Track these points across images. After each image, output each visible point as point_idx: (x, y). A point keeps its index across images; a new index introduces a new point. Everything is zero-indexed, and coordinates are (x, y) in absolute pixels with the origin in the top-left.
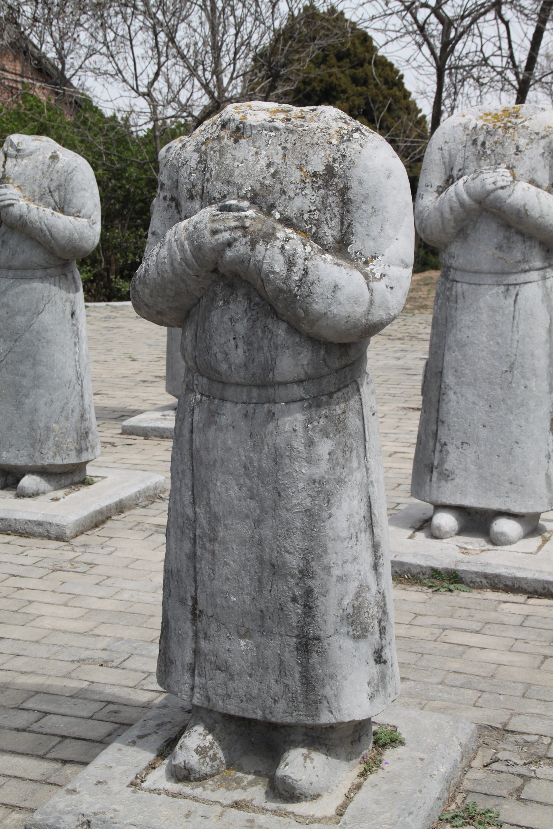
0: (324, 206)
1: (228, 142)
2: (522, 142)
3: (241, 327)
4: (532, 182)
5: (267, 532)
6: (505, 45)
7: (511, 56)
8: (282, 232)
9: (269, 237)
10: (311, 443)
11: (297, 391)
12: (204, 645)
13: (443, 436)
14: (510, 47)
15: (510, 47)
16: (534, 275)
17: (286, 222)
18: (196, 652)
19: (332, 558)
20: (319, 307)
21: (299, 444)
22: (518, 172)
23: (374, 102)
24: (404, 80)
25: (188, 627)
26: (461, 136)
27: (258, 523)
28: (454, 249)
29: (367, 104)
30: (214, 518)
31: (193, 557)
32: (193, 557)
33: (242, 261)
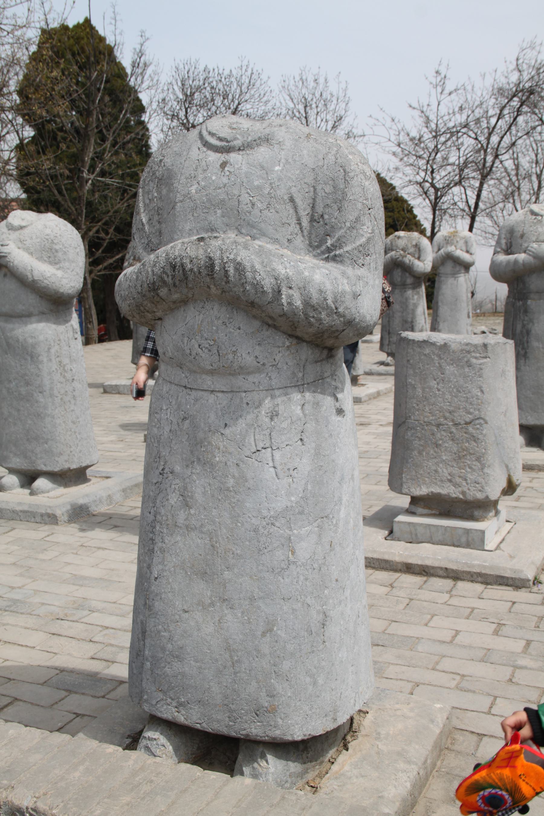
0: (415, 251)
1: (396, 239)
2: (458, 239)
3: (400, 274)
4: (461, 250)
5: (404, 314)
6: (464, 196)
7: (467, 202)
8: (408, 256)
9: (406, 256)
10: (413, 296)
11: (410, 286)
12: (391, 339)
13: (438, 320)
14: (466, 198)
15: (466, 198)
16: (462, 275)
17: (408, 254)
18: (389, 341)
19: (417, 319)
20: (415, 269)
21: (411, 296)
22: (458, 247)
23: (398, 221)
24: (414, 209)
25: (387, 336)
26: (442, 238)
27: (403, 313)
28: (441, 268)
29: (394, 221)
30: (393, 313)
31: (389, 321)
32: (389, 321)
33: (401, 261)
